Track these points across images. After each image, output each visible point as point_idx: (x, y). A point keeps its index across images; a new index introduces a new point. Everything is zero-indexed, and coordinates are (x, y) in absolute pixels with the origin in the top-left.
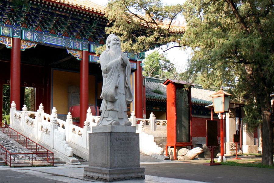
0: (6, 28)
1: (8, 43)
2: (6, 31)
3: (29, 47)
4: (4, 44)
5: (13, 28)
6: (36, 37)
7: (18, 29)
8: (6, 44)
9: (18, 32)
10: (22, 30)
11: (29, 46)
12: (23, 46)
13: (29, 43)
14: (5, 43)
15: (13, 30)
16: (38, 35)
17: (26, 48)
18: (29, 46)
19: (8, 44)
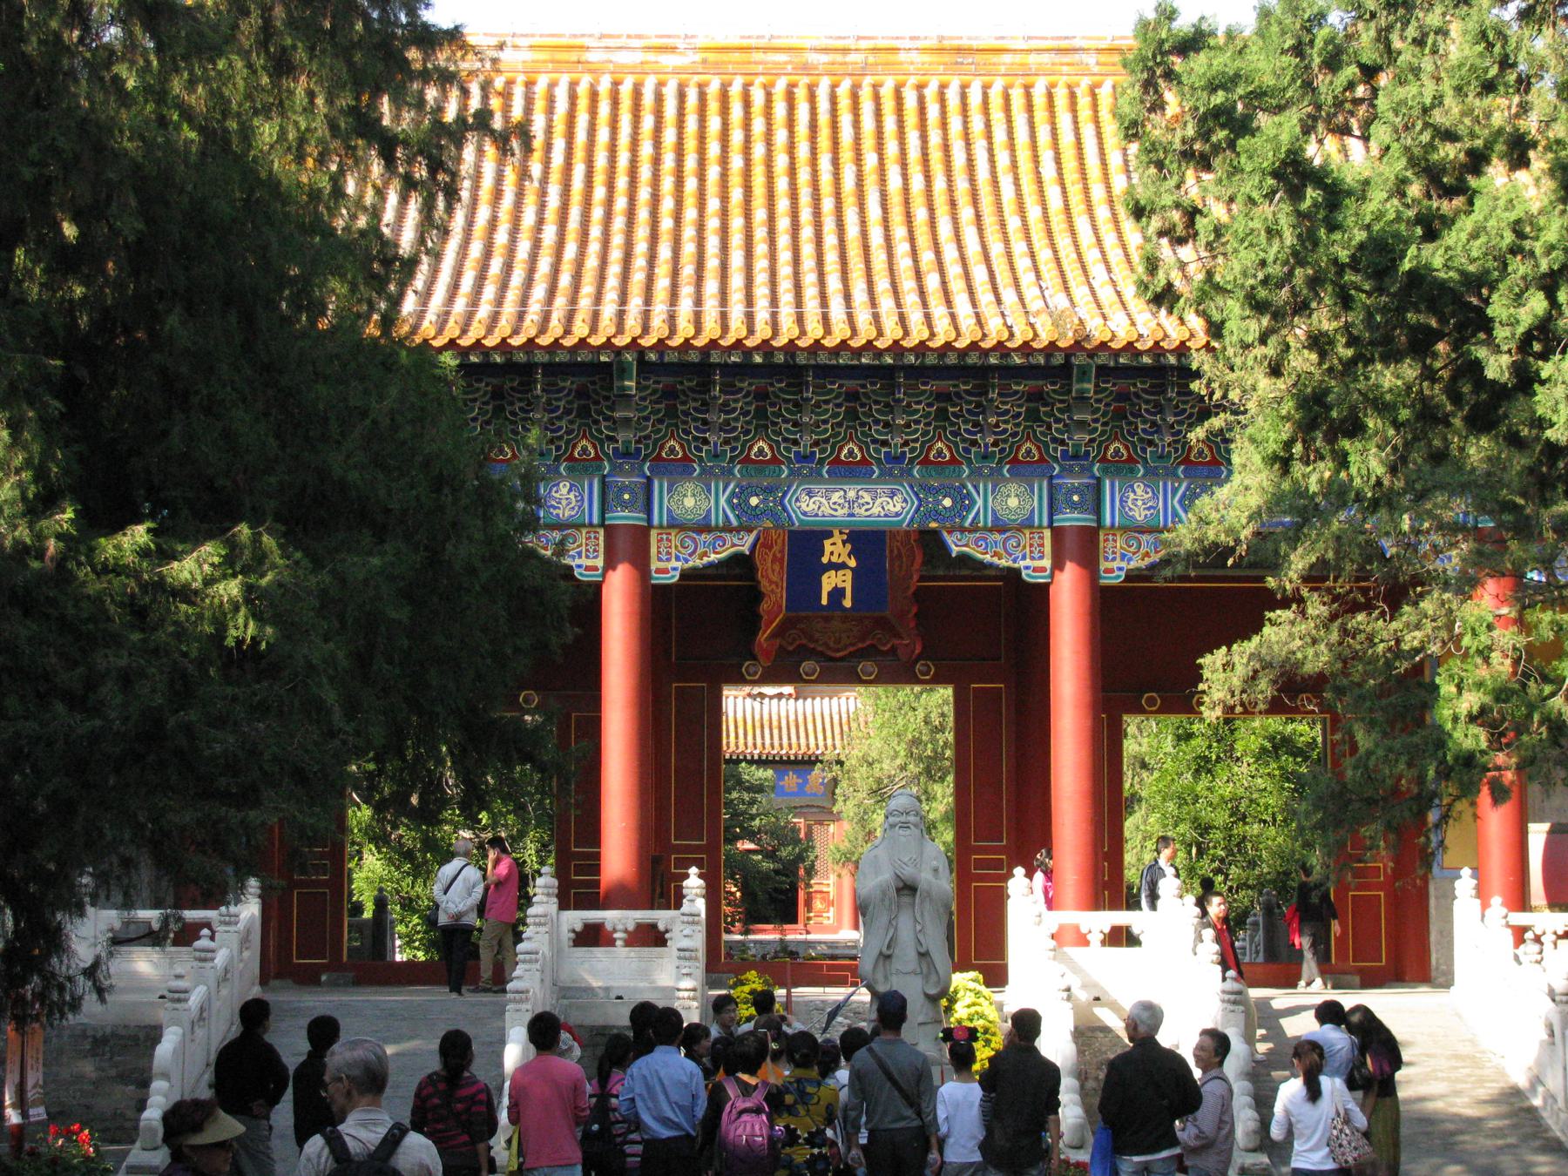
0: (1013, 488)
1: (1032, 558)
2: (1013, 502)
3: (1147, 561)
4: (1010, 564)
5: (1051, 478)
6: (1180, 502)
7: (1076, 482)
8: (1022, 564)
9: (1076, 498)
10: (1098, 479)
11: (1147, 555)
12: (1114, 559)
13: (1144, 538)
14: (1015, 561)
15: (1051, 487)
16: (1188, 488)
17: (1133, 565)
18: (1147, 555)
19: (1028, 562)
